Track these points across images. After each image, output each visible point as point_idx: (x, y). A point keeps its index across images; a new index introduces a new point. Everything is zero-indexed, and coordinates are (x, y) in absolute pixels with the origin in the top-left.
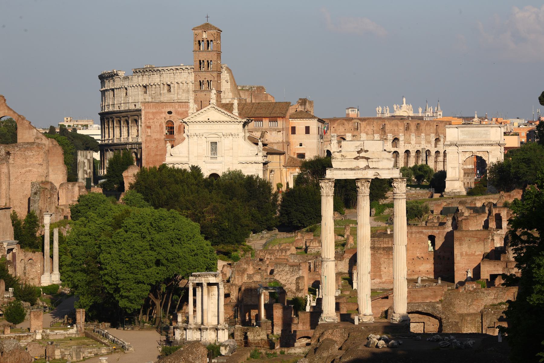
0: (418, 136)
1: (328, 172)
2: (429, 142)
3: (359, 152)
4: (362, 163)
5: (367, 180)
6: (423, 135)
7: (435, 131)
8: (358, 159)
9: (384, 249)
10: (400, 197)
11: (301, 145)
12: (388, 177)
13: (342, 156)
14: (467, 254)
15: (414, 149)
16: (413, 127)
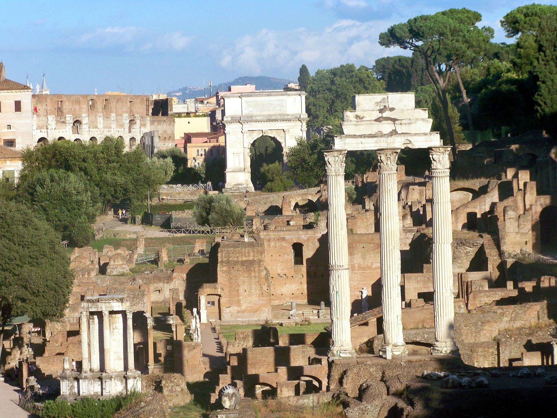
0: (107, 117)
1: (337, 140)
2: (122, 126)
3: (381, 111)
4: (387, 127)
5: (394, 150)
6: (113, 115)
7: (129, 110)
8: (380, 121)
9: (243, 263)
10: (443, 175)
11: (9, 127)
12: (425, 146)
13: (357, 117)
14: (360, 268)
15: (101, 136)
16: (100, 105)
